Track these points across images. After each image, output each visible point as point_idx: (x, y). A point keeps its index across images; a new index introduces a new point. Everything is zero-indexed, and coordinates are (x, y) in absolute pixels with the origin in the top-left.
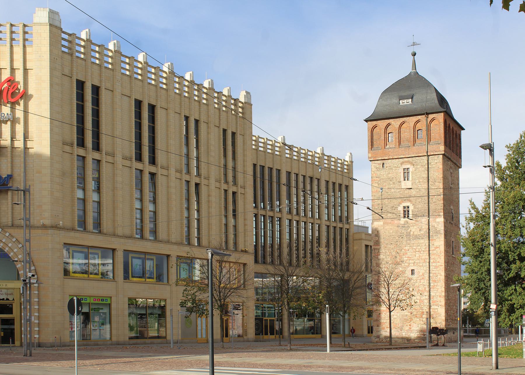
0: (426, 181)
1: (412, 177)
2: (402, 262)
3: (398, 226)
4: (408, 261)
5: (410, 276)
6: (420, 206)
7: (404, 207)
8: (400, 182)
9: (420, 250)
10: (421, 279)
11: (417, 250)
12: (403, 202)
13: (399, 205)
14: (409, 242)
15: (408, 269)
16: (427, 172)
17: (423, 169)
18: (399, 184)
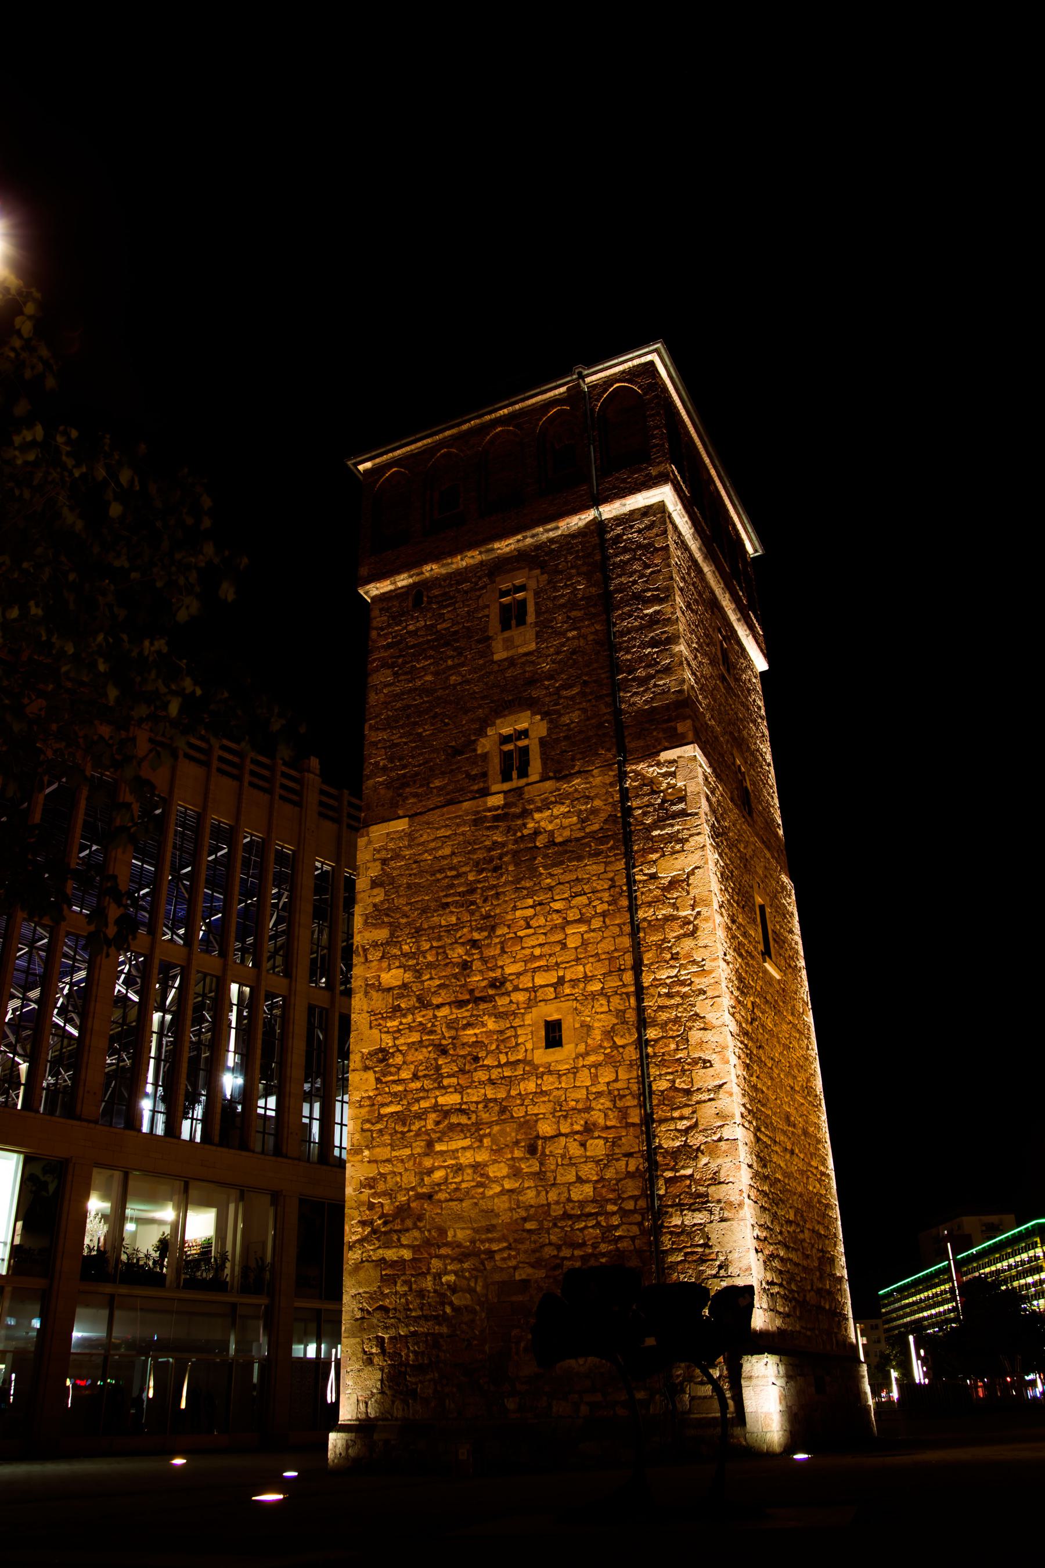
4: (525, 982)
5: (542, 1056)
9: (589, 912)
10: (596, 1066)
11: (572, 915)
15: (528, 1019)
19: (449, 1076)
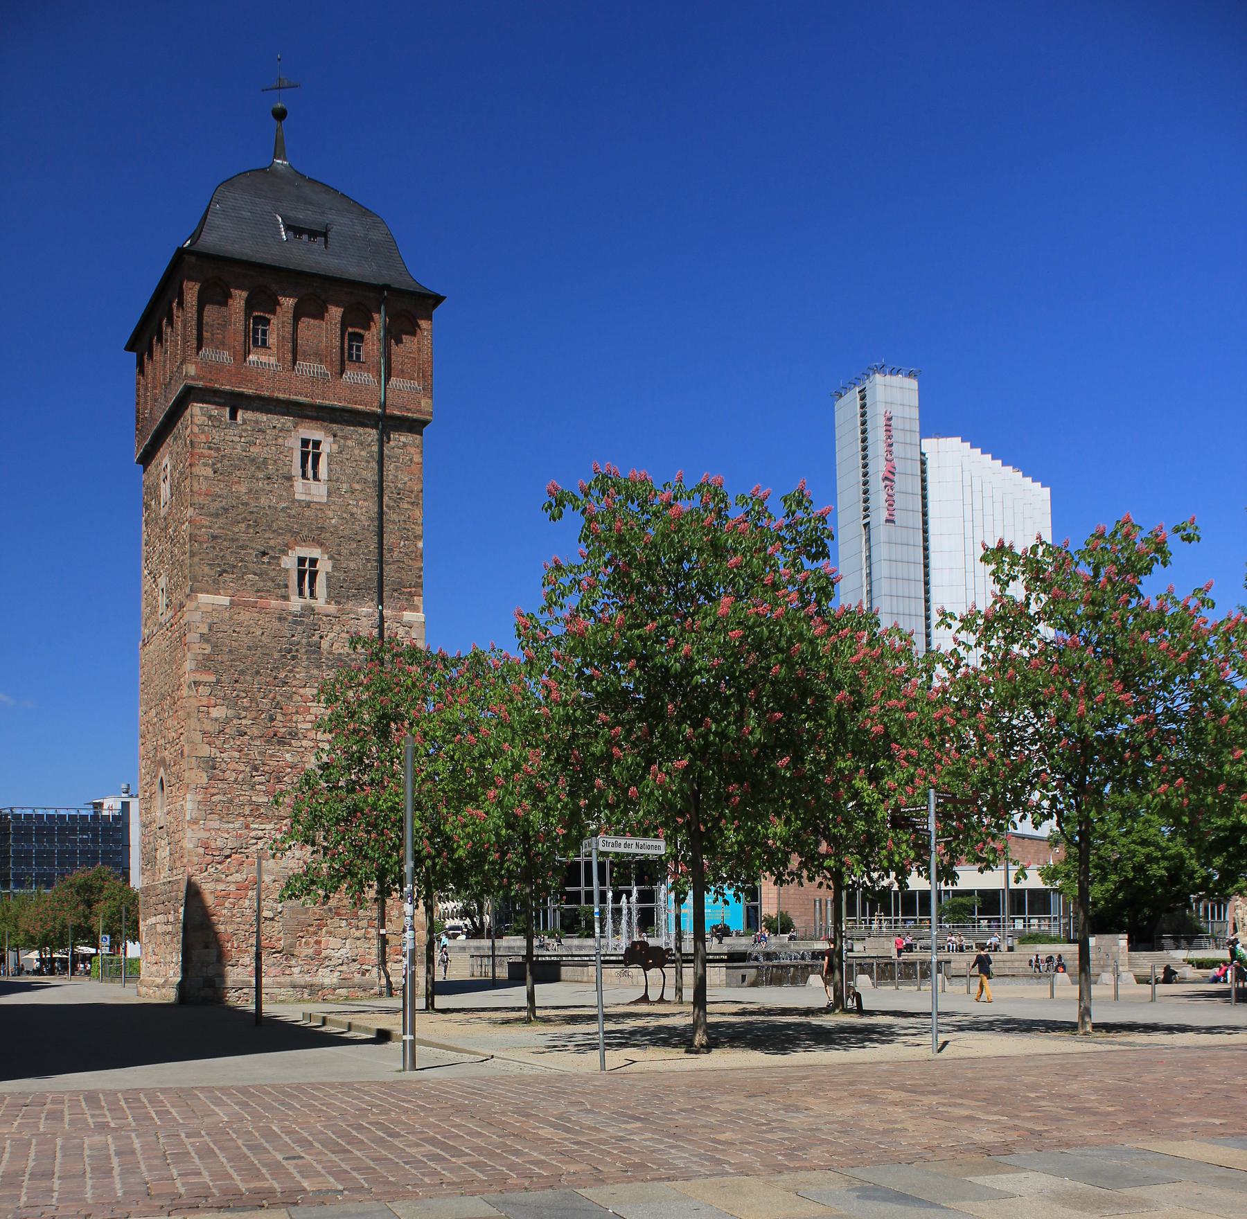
0: (372, 491)
1: (330, 470)
2: (294, 735)
3: (280, 619)
6: (352, 565)
7: (301, 561)
8: (289, 478)
12: (297, 544)
13: (285, 552)
14: (315, 672)
16: (374, 465)
17: (363, 453)
18: (287, 484)
19: (260, 784)
